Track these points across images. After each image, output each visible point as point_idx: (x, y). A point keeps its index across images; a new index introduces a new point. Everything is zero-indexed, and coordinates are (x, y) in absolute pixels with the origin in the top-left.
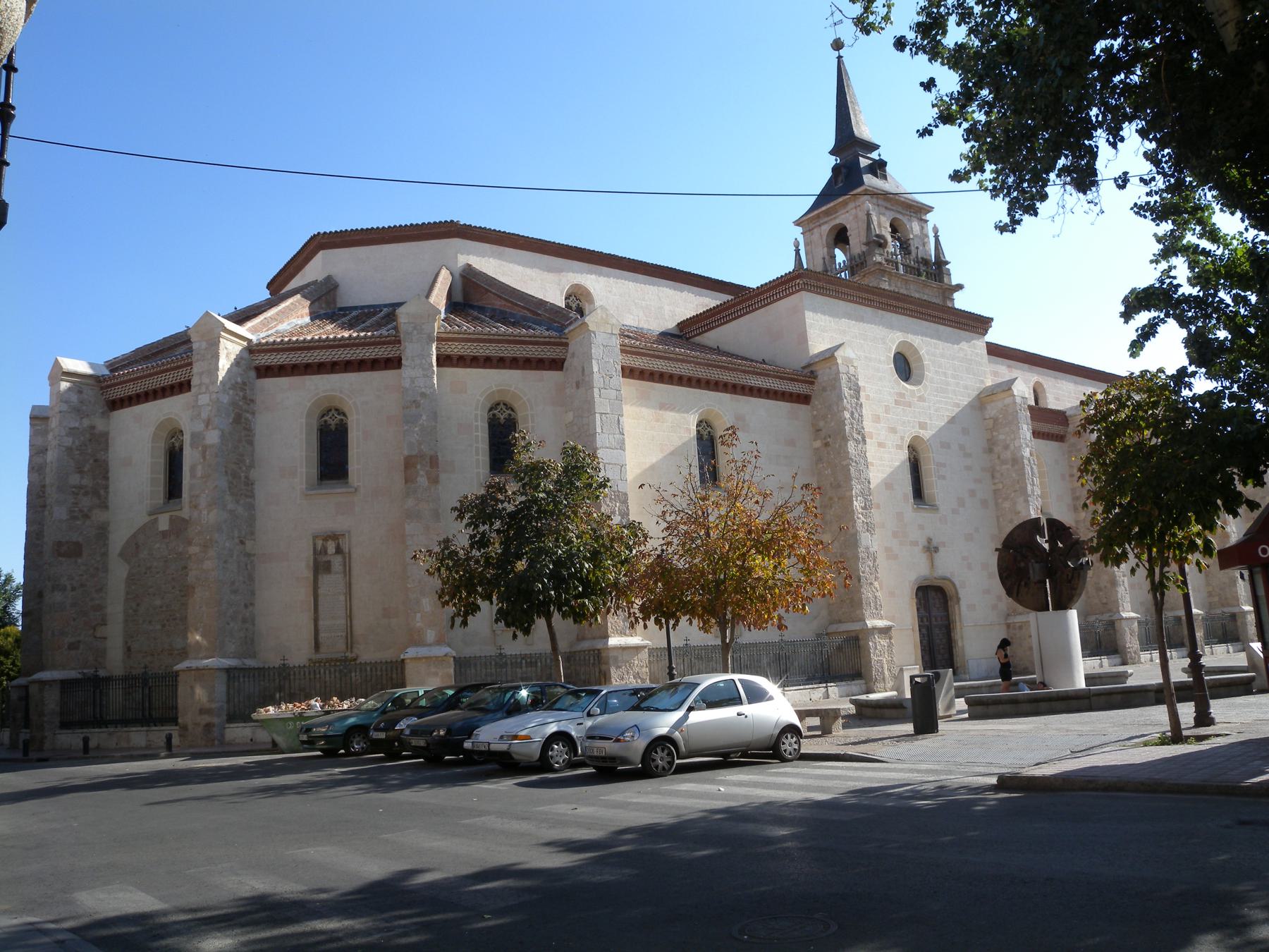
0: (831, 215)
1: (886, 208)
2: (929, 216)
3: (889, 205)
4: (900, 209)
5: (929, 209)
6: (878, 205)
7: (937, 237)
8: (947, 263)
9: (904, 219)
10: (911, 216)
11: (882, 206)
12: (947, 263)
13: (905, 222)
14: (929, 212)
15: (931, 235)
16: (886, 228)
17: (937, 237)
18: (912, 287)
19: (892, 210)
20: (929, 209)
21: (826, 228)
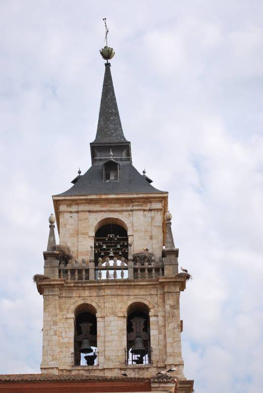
9: (124, 218)
16: (87, 234)
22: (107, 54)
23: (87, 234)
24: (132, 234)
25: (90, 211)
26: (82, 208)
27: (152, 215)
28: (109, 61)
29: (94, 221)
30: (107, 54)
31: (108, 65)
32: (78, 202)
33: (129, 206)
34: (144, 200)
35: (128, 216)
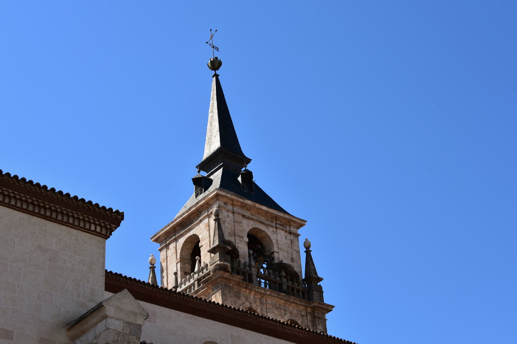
0: (187, 226)
1: (243, 216)
2: (299, 231)
3: (248, 214)
4: (263, 219)
5: (301, 224)
6: (233, 213)
7: (308, 252)
8: (320, 279)
9: (269, 231)
10: (276, 228)
11: (239, 214)
12: (320, 279)
13: (269, 234)
14: (301, 225)
15: (302, 250)
16: (242, 237)
17: (308, 252)
18: (269, 301)
19: (252, 219)
20: (301, 224)
21: (182, 241)
22: (216, 65)
23: (242, 237)
24: (278, 252)
25: (243, 216)
26: (236, 209)
27: (292, 238)
28: (218, 72)
29: (247, 226)
30: (216, 65)
31: (216, 76)
32: (235, 203)
33: (273, 222)
34: (286, 221)
35: (272, 232)
